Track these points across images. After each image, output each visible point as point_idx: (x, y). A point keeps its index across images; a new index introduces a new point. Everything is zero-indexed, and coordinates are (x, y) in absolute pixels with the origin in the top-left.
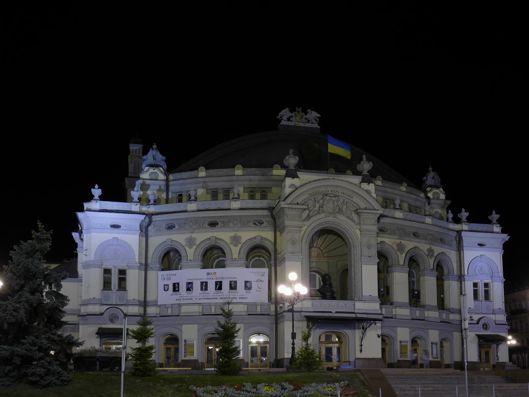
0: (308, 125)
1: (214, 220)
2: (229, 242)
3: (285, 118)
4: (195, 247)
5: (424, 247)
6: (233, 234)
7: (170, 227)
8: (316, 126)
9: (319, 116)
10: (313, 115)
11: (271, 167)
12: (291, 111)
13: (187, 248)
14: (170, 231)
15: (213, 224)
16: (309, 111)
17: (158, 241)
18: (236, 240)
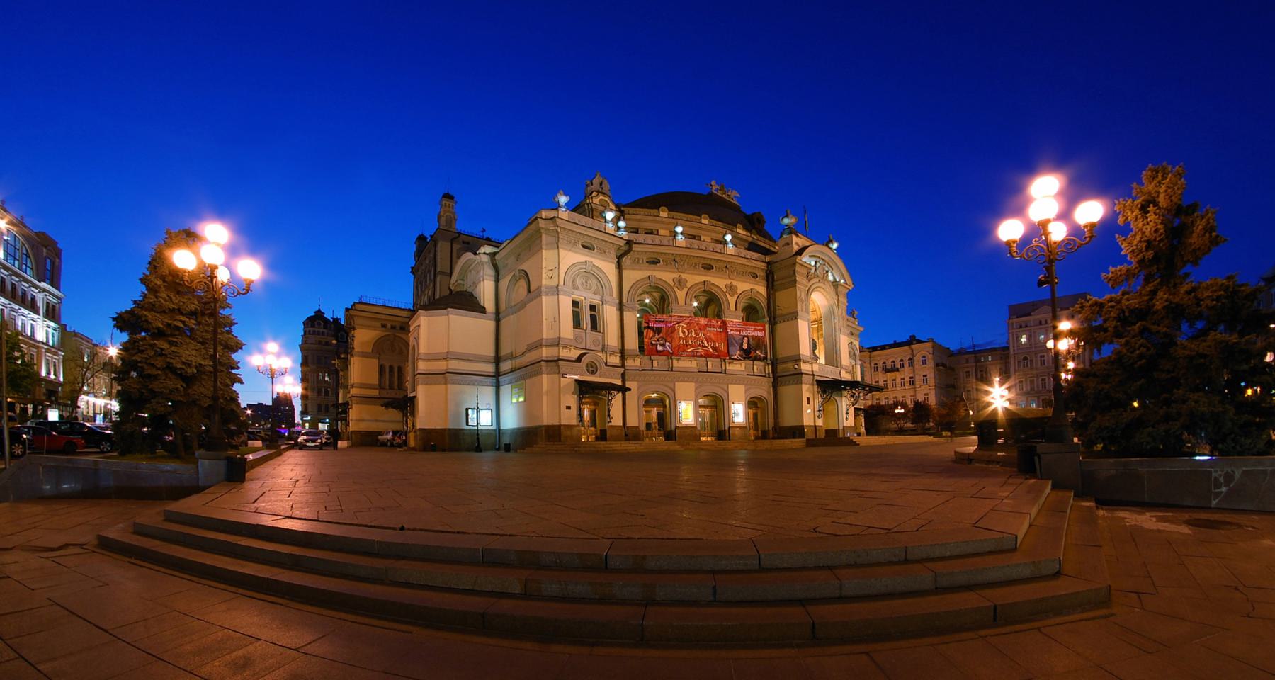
4: (685, 290)
6: (728, 282)
7: (654, 262)
15: (708, 268)
18: (732, 288)
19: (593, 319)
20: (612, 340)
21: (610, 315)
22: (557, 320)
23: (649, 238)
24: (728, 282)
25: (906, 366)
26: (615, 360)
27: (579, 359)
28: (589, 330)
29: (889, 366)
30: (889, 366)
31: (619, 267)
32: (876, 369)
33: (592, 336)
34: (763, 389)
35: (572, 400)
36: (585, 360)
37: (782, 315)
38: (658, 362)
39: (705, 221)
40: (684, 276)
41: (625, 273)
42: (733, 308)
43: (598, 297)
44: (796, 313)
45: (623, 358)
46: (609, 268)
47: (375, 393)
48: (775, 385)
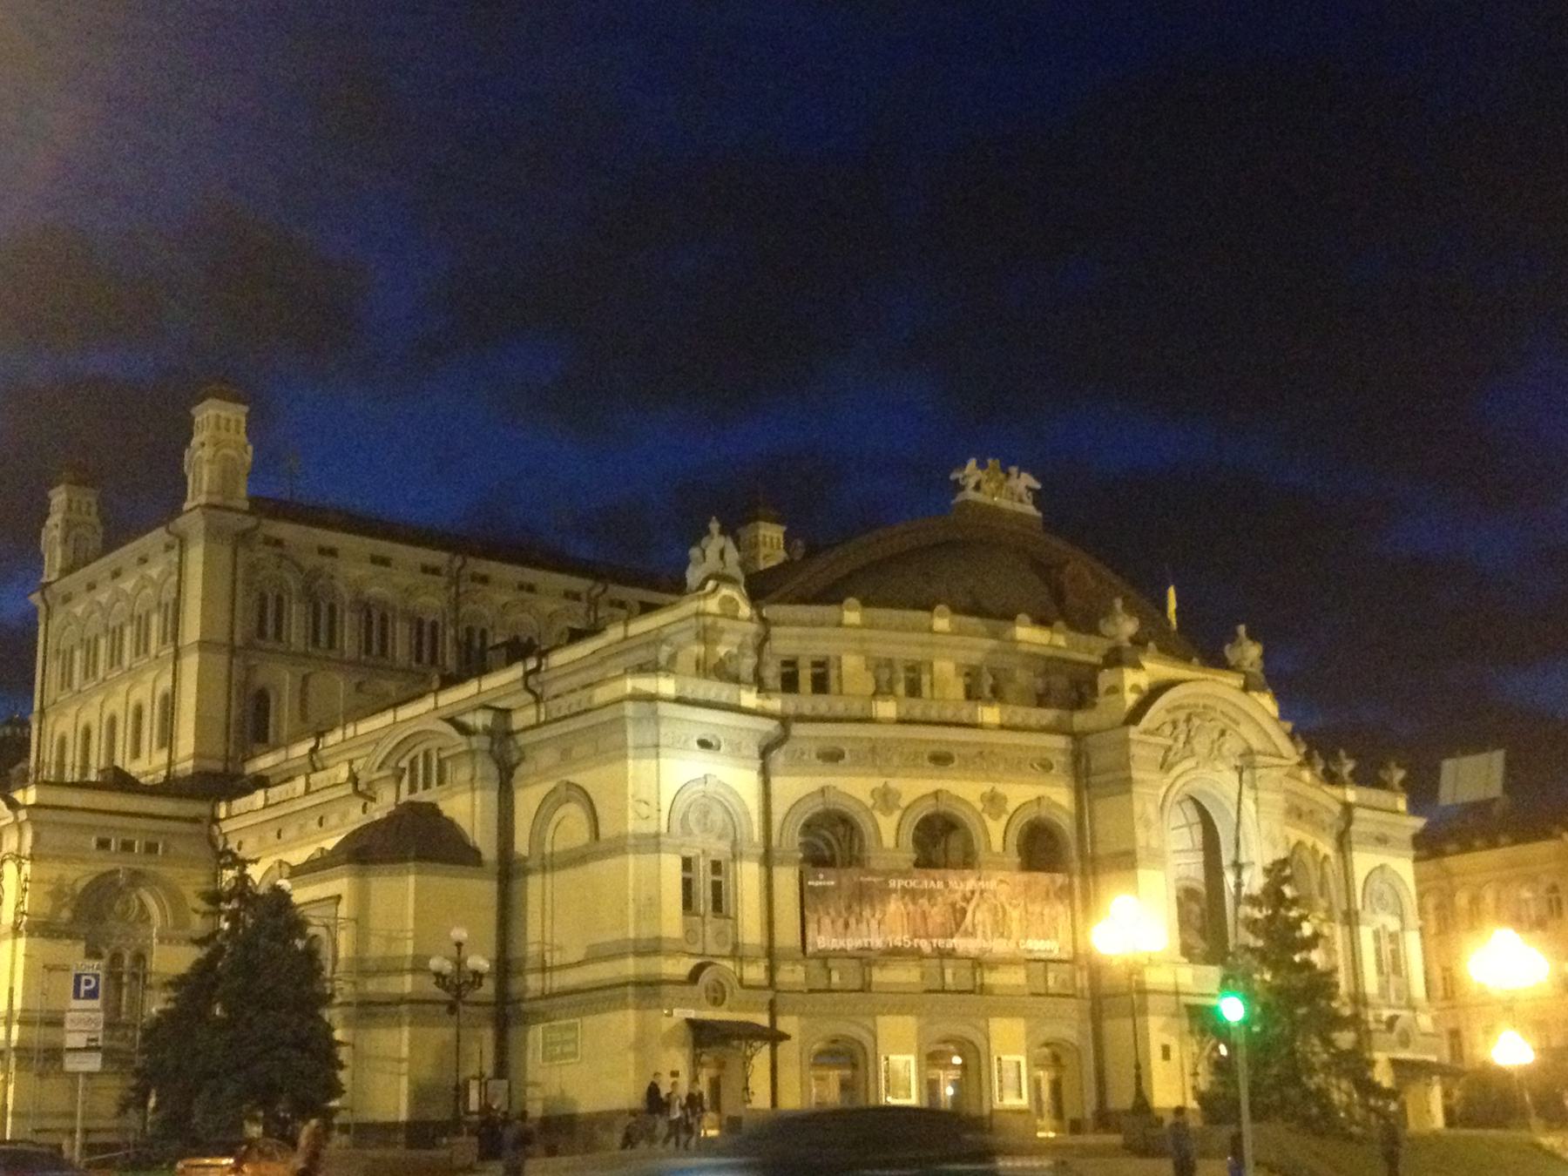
0: (1019, 507)
1: (944, 749)
2: (979, 806)
3: (972, 482)
4: (897, 814)
5: (1309, 840)
6: (986, 787)
7: (832, 756)
8: (1030, 509)
9: (1038, 486)
10: (1024, 481)
11: (1010, 617)
12: (982, 465)
13: (877, 814)
14: (829, 766)
15: (941, 759)
16: (1014, 470)
17: (795, 787)
18: (994, 801)
19: (717, 886)
20: (751, 930)
21: (748, 876)
22: (652, 905)
23: (822, 704)
24: (986, 787)
26: (755, 973)
27: (694, 976)
28: (709, 917)
31: (765, 773)
33: (711, 926)
36: (706, 977)
39: (942, 623)
41: (777, 783)
45: (771, 970)
46: (742, 781)
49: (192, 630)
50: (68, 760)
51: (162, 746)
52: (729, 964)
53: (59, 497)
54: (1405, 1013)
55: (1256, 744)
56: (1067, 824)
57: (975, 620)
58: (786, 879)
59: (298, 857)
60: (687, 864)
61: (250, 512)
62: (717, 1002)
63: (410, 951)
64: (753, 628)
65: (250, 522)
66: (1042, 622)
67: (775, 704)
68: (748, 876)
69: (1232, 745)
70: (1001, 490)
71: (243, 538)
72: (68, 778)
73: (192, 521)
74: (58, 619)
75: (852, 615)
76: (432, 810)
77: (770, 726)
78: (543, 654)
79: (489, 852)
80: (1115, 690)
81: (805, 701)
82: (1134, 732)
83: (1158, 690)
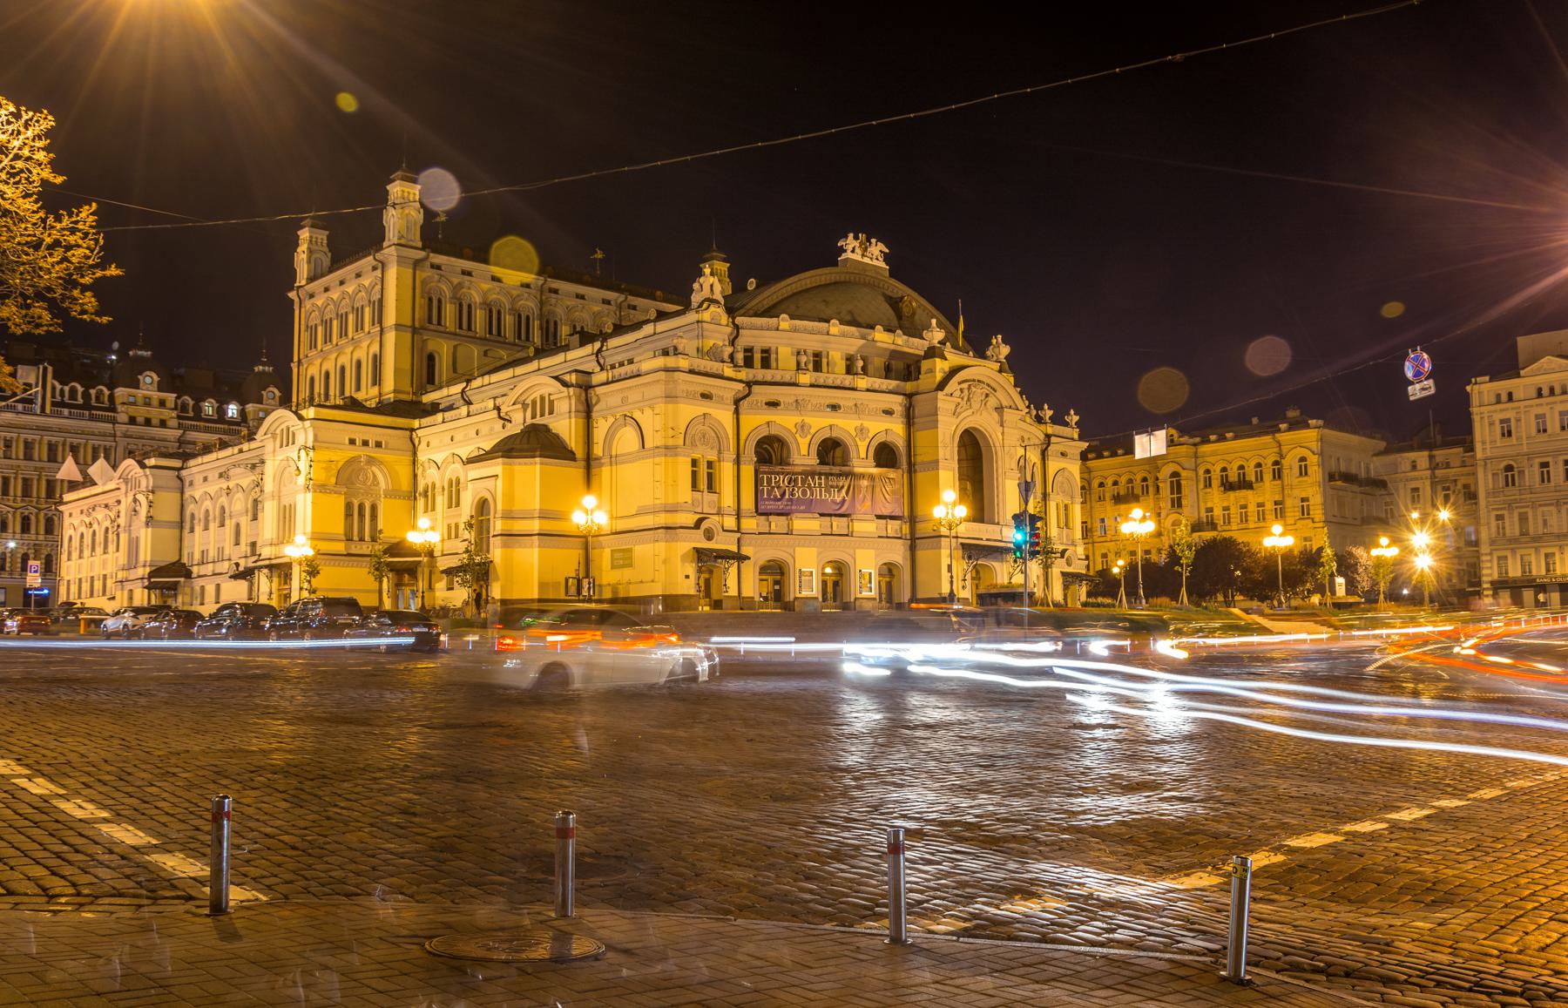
0: (875, 263)
3: (850, 248)
6: (858, 423)
8: (882, 264)
12: (856, 238)
19: (710, 476)
23: (768, 375)
25: (1268, 476)
26: (730, 522)
27: (697, 525)
29: (1233, 477)
30: (1233, 477)
31: (737, 412)
32: (1208, 484)
33: (708, 497)
34: (897, 553)
35: (691, 569)
36: (704, 525)
37: (923, 463)
38: (777, 523)
40: (807, 420)
42: (863, 455)
43: (715, 452)
44: (937, 462)
46: (725, 416)
47: (340, 547)
48: (912, 549)
49: (390, 318)
50: (316, 390)
51: (374, 384)
52: (716, 518)
53: (304, 234)
54: (1071, 548)
55: (1005, 403)
56: (900, 442)
57: (853, 329)
58: (748, 471)
59: (466, 451)
60: (694, 463)
61: (423, 249)
62: (709, 538)
63: (537, 507)
64: (729, 330)
65: (422, 254)
66: (889, 330)
67: (744, 374)
68: (727, 471)
69: (992, 402)
70: (864, 254)
71: (417, 264)
72: (332, 402)
73: (389, 252)
74: (308, 304)
75: (785, 322)
76: (546, 428)
77: (741, 386)
78: (604, 340)
79: (580, 454)
80: (932, 371)
81: (759, 373)
82: (940, 394)
83: (954, 371)
